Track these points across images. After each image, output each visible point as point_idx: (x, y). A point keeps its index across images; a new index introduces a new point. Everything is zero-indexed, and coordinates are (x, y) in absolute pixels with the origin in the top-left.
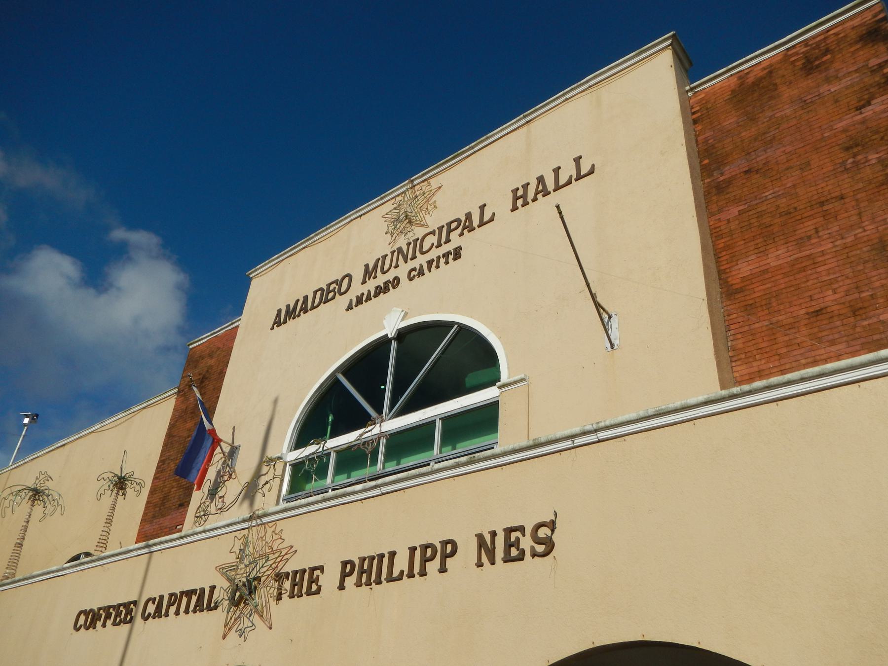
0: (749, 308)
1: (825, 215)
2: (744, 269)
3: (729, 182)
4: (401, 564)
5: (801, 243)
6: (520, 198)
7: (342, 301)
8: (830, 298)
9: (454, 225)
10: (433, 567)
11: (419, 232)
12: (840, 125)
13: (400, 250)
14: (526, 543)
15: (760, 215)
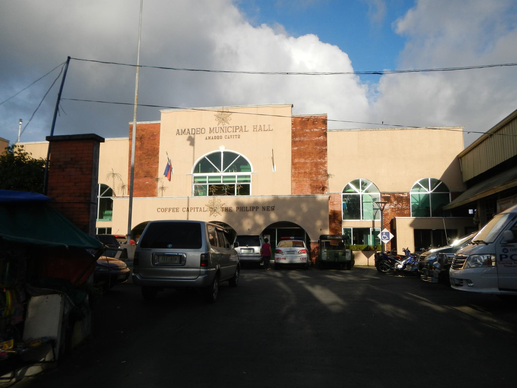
0: (295, 168)
1: (310, 155)
2: (296, 161)
3: (297, 141)
4: (248, 209)
5: (305, 159)
6: (255, 129)
7: (204, 136)
8: (307, 170)
9: (237, 128)
10: (255, 210)
11: (227, 125)
12: (315, 139)
13: (221, 128)
14: (270, 209)
15: (300, 151)
